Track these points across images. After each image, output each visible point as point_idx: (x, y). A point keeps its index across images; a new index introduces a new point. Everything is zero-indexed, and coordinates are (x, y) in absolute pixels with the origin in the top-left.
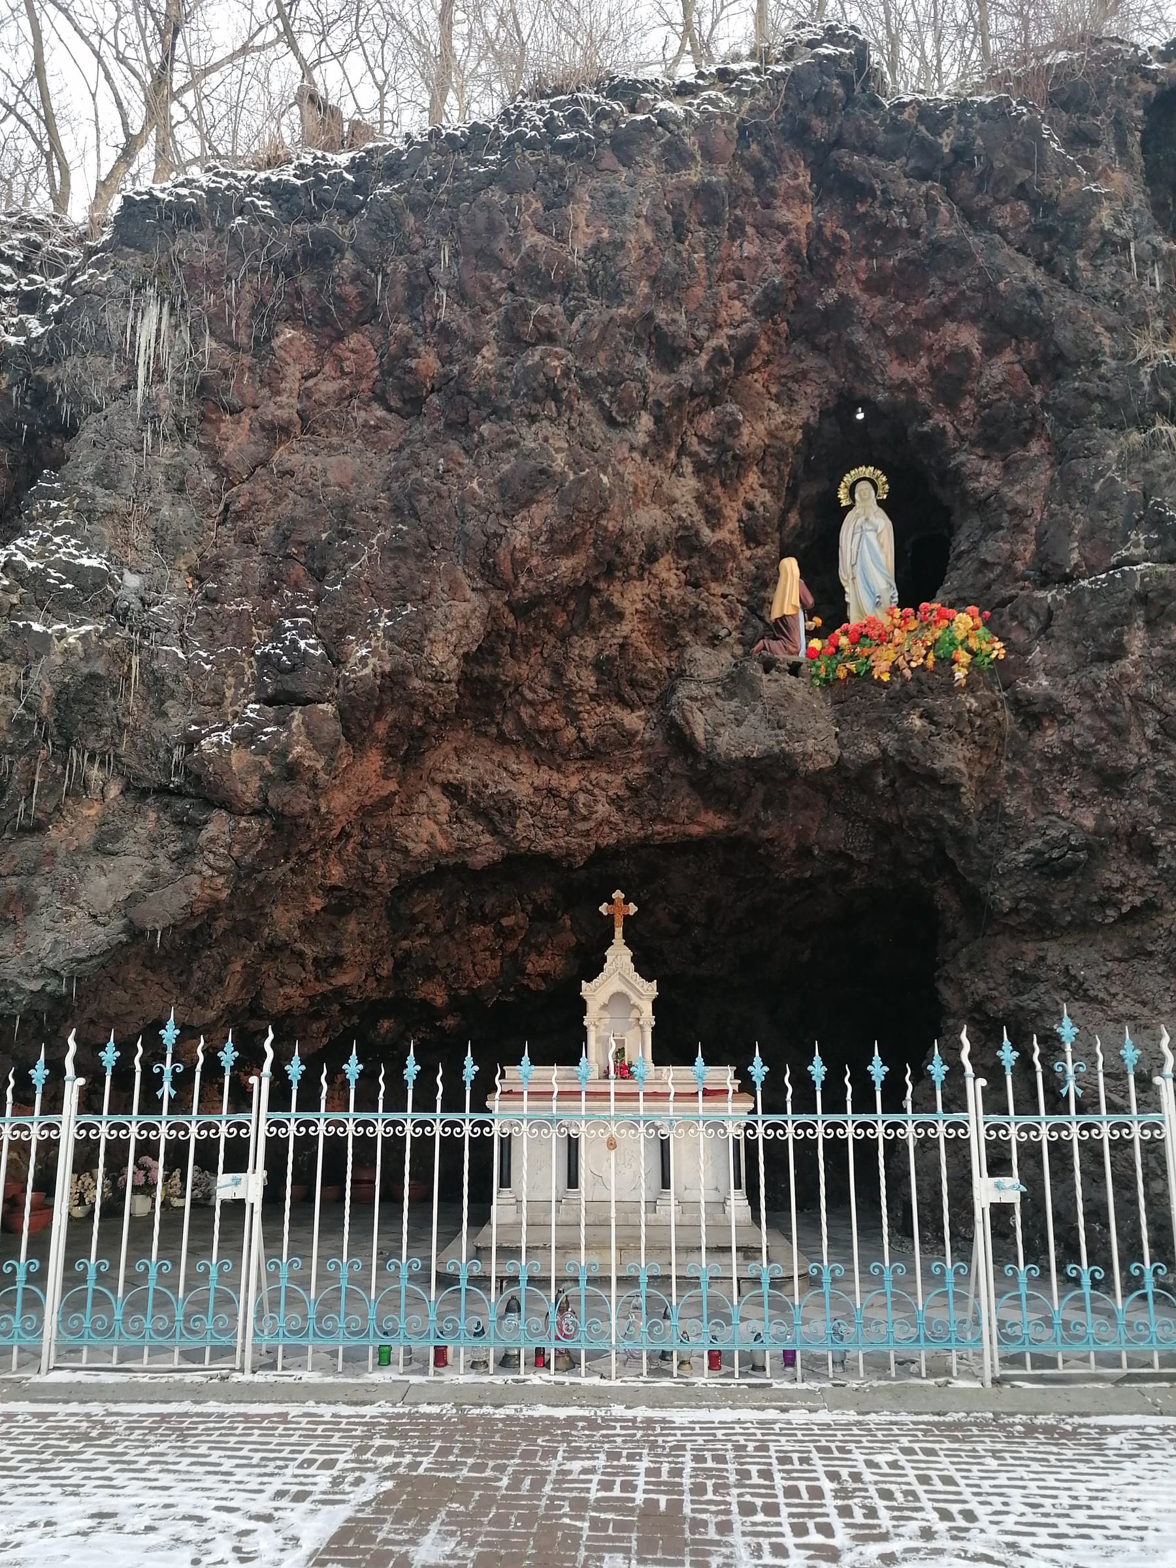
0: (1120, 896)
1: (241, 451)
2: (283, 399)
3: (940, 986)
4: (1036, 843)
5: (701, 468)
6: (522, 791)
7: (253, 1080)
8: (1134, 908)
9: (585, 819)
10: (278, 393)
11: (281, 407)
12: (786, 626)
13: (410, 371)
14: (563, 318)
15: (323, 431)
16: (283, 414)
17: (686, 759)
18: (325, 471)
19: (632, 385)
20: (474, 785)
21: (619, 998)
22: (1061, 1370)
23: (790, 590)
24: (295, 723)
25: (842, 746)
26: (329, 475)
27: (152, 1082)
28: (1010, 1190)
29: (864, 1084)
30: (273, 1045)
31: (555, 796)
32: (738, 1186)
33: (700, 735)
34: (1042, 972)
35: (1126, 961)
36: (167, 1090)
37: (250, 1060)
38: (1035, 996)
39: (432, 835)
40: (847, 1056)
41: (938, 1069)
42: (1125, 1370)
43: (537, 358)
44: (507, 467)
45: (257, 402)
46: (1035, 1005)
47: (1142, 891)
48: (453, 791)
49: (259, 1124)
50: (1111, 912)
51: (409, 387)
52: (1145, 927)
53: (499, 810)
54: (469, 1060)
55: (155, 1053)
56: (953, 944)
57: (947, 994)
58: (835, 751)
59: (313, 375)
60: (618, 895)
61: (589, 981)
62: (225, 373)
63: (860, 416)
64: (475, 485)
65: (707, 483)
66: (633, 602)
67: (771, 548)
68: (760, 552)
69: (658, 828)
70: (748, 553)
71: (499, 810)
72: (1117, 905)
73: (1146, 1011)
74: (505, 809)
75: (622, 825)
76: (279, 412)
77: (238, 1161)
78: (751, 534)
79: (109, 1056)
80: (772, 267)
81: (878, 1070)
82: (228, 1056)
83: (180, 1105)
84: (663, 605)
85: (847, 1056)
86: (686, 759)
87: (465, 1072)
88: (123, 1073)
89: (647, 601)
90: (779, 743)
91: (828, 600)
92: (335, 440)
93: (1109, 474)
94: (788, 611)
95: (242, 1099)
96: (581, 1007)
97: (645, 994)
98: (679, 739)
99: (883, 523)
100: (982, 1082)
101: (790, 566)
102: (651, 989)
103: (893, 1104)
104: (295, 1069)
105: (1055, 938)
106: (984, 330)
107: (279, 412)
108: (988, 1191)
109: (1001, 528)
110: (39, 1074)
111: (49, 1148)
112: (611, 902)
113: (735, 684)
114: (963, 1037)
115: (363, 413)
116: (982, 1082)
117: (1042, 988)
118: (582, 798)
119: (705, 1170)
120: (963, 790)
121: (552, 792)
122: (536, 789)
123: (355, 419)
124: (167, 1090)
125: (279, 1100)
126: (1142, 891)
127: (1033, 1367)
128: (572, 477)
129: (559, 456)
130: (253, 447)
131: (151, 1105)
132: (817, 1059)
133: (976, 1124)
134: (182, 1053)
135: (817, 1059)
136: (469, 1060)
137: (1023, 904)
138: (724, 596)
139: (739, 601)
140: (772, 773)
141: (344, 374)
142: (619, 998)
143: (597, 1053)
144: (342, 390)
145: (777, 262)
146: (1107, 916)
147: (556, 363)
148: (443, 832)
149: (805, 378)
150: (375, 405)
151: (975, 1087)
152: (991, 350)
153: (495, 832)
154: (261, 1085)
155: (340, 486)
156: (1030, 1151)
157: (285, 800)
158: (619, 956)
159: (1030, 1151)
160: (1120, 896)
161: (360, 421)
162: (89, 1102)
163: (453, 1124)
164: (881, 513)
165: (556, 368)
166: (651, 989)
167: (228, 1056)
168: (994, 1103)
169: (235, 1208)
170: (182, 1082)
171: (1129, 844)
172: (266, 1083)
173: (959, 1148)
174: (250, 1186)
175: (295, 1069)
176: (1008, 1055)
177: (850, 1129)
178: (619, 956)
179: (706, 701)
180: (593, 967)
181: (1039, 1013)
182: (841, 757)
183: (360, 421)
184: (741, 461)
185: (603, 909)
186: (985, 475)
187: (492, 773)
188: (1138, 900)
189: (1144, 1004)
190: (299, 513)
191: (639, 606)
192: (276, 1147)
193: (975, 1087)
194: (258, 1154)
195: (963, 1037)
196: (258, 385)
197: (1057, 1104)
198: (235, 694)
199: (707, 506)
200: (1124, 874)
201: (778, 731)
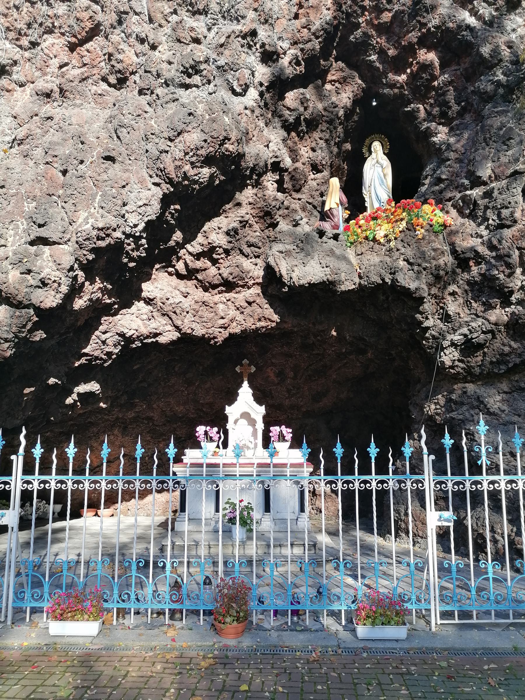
0: (508, 358)
1: (25, 107)
2: (48, 77)
3: (411, 408)
4: (465, 330)
7: (13, 457)
8: (515, 365)
9: (222, 318)
10: (45, 74)
11: (47, 82)
12: (332, 214)
13: (120, 61)
14: (205, 30)
15: (72, 96)
16: (49, 86)
17: (277, 286)
18: (70, 117)
19: (245, 71)
20: (161, 299)
22: (475, 621)
23: (335, 198)
24: (45, 256)
25: (360, 277)
26: (72, 119)
29: (365, 458)
30: (26, 437)
31: (206, 306)
33: (284, 272)
34: (465, 400)
35: (510, 393)
38: (461, 412)
39: (139, 326)
40: (356, 444)
41: (408, 450)
42: (511, 621)
43: (189, 50)
44: (171, 112)
45: (34, 79)
46: (461, 417)
47: (520, 355)
50: (503, 367)
51: (120, 71)
52: (521, 375)
53: (175, 312)
54: (139, 446)
56: (418, 386)
58: (357, 280)
59: (66, 64)
60: (245, 361)
61: (230, 405)
62: (15, 63)
63: (374, 104)
64: (153, 122)
65: (289, 134)
66: (248, 198)
67: (326, 173)
68: (319, 175)
69: (263, 324)
70: (312, 176)
71: (175, 312)
72: (506, 363)
73: (520, 419)
74: (178, 312)
75: (243, 322)
76: (46, 85)
80: (325, 12)
81: (373, 451)
84: (264, 200)
85: (356, 444)
86: (277, 286)
87: (137, 452)
89: (255, 197)
90: (326, 275)
91: (355, 203)
92: (78, 102)
93: (509, 125)
94: (334, 206)
96: (225, 419)
97: (259, 412)
99: (386, 162)
100: (432, 457)
101: (335, 182)
102: (262, 410)
103: (382, 469)
104: (38, 451)
105: (472, 382)
106: (441, 52)
107: (46, 85)
109: (449, 160)
112: (242, 365)
114: (422, 432)
115: (94, 87)
116: (432, 457)
117: (465, 408)
118: (221, 306)
120: (425, 300)
122: (197, 302)
123: (90, 90)
125: (28, 470)
126: (520, 355)
127: (459, 619)
128: (207, 117)
129: (200, 106)
130: (31, 105)
132: (339, 445)
135: (339, 445)
136: (139, 446)
137: (457, 363)
138: (299, 199)
139: (307, 202)
141: (85, 65)
144: (82, 74)
145: (328, 9)
146: (500, 369)
147: (200, 54)
148: (144, 324)
149: (344, 81)
150: (101, 83)
151: (428, 460)
154: (18, 462)
155: (78, 125)
156: (460, 496)
157: (41, 299)
158: (245, 392)
159: (460, 496)
160: (508, 358)
161: (93, 91)
163: (129, 482)
164: (385, 157)
165: (200, 57)
166: (262, 410)
168: (439, 469)
171: (514, 330)
172: (21, 459)
173: (420, 496)
176: (448, 441)
177: (357, 484)
178: (245, 392)
180: (231, 397)
181: (463, 421)
182: (360, 284)
183: (93, 91)
185: (238, 369)
187: (172, 292)
188: (518, 360)
189: (519, 416)
190: (55, 139)
191: (251, 200)
193: (428, 460)
195: (422, 432)
196: (34, 70)
197: (476, 469)
198: (14, 240)
199: (290, 148)
200: (510, 346)
201: (325, 269)
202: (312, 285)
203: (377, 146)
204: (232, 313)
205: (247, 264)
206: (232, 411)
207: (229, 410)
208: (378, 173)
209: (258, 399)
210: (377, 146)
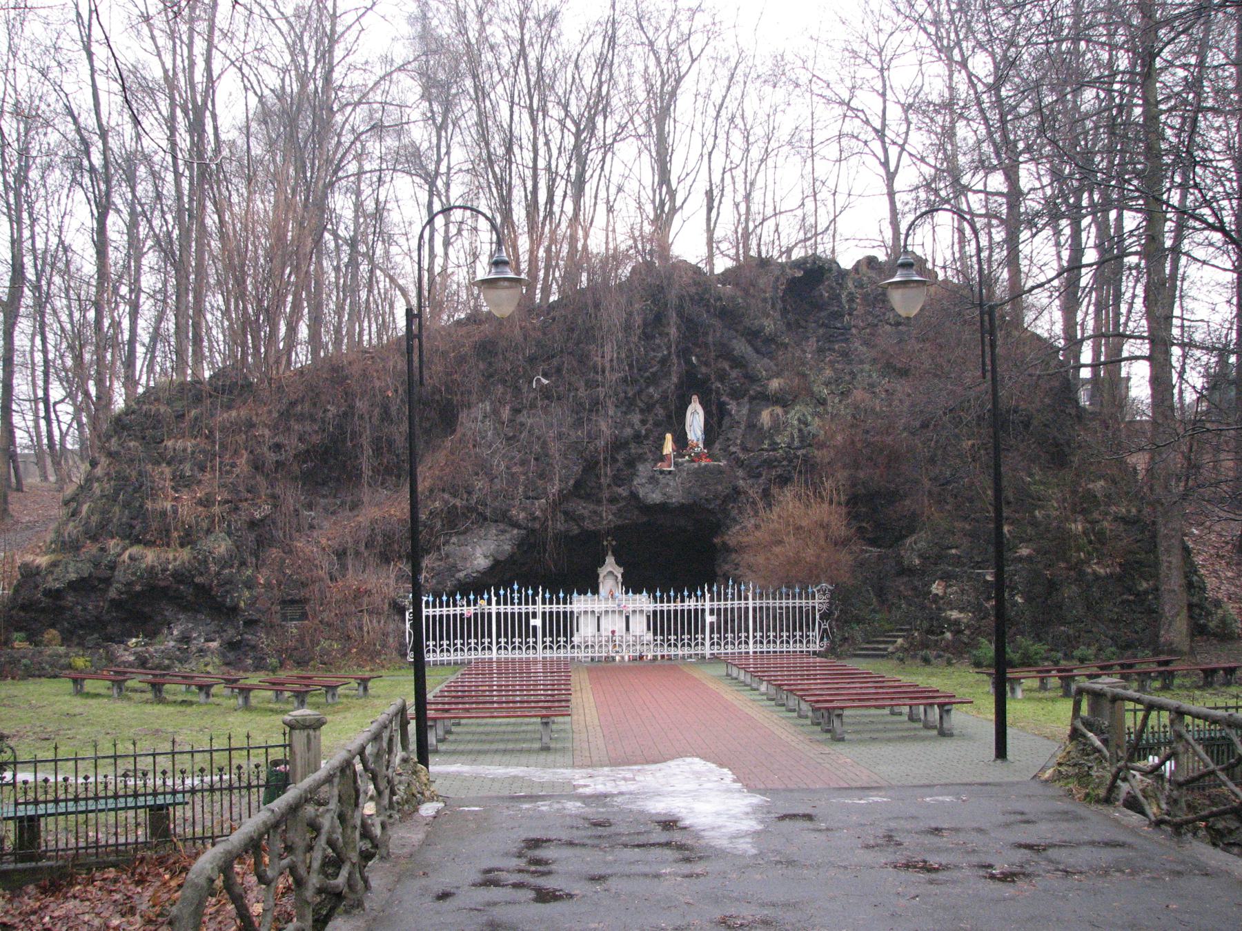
5: (642, 411)
6: (586, 513)
21: (610, 572)
27: (512, 599)
28: (714, 618)
32: (649, 629)
36: (516, 601)
37: (536, 593)
41: (699, 593)
48: (566, 513)
49: (539, 608)
55: (512, 591)
57: (717, 570)
77: (534, 615)
78: (657, 424)
79: (502, 592)
82: (530, 592)
83: (520, 603)
88: (505, 595)
91: (681, 441)
95: (534, 603)
96: (598, 576)
97: (619, 572)
98: (634, 496)
101: (669, 436)
102: (621, 570)
104: (547, 595)
108: (709, 619)
110: (486, 596)
111: (490, 614)
113: (652, 480)
119: (639, 625)
121: (595, 512)
124: (516, 601)
125: (544, 602)
131: (513, 604)
133: (708, 605)
134: (519, 591)
140: (663, 508)
142: (610, 572)
143: (604, 590)
151: (708, 596)
152: (732, 368)
153: (578, 525)
154: (539, 599)
156: (719, 610)
158: (610, 559)
159: (719, 610)
162: (498, 603)
166: (621, 570)
167: (530, 592)
169: (535, 628)
170: (520, 599)
173: (703, 611)
174: (537, 622)
175: (547, 595)
178: (610, 559)
179: (642, 485)
180: (602, 563)
184: (653, 405)
186: (732, 406)
192: (544, 614)
194: (540, 615)
202: (656, 505)
203: (695, 398)
204: (610, 517)
205: (620, 490)
206: (603, 572)
207: (600, 570)
208: (695, 420)
209: (618, 563)
210: (695, 398)
